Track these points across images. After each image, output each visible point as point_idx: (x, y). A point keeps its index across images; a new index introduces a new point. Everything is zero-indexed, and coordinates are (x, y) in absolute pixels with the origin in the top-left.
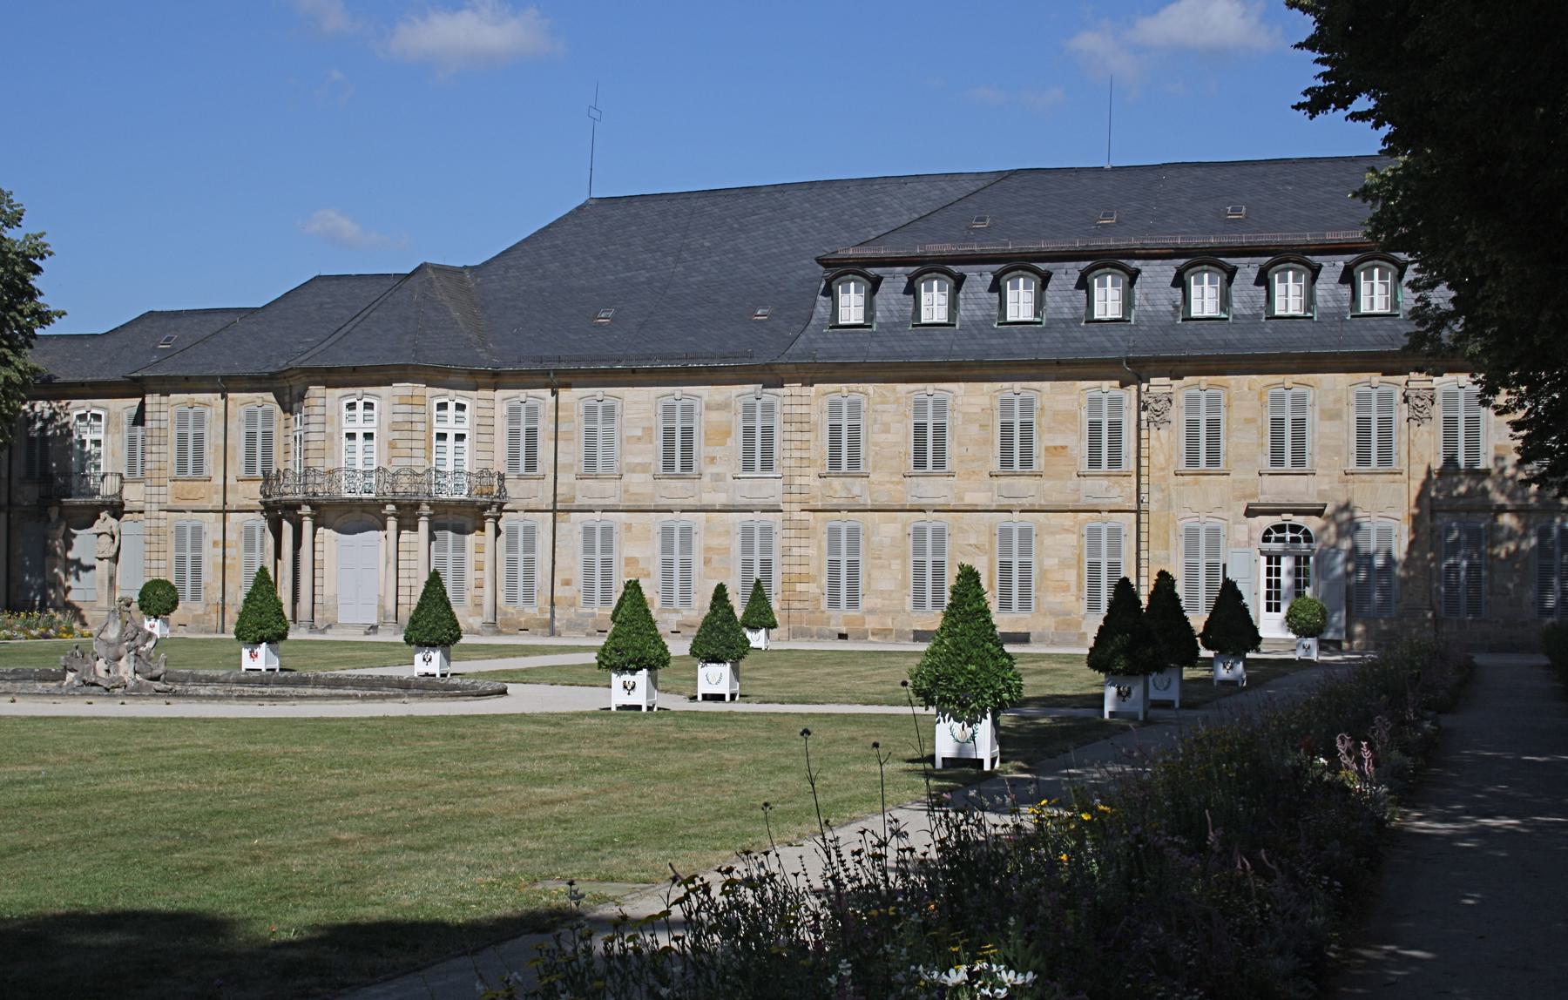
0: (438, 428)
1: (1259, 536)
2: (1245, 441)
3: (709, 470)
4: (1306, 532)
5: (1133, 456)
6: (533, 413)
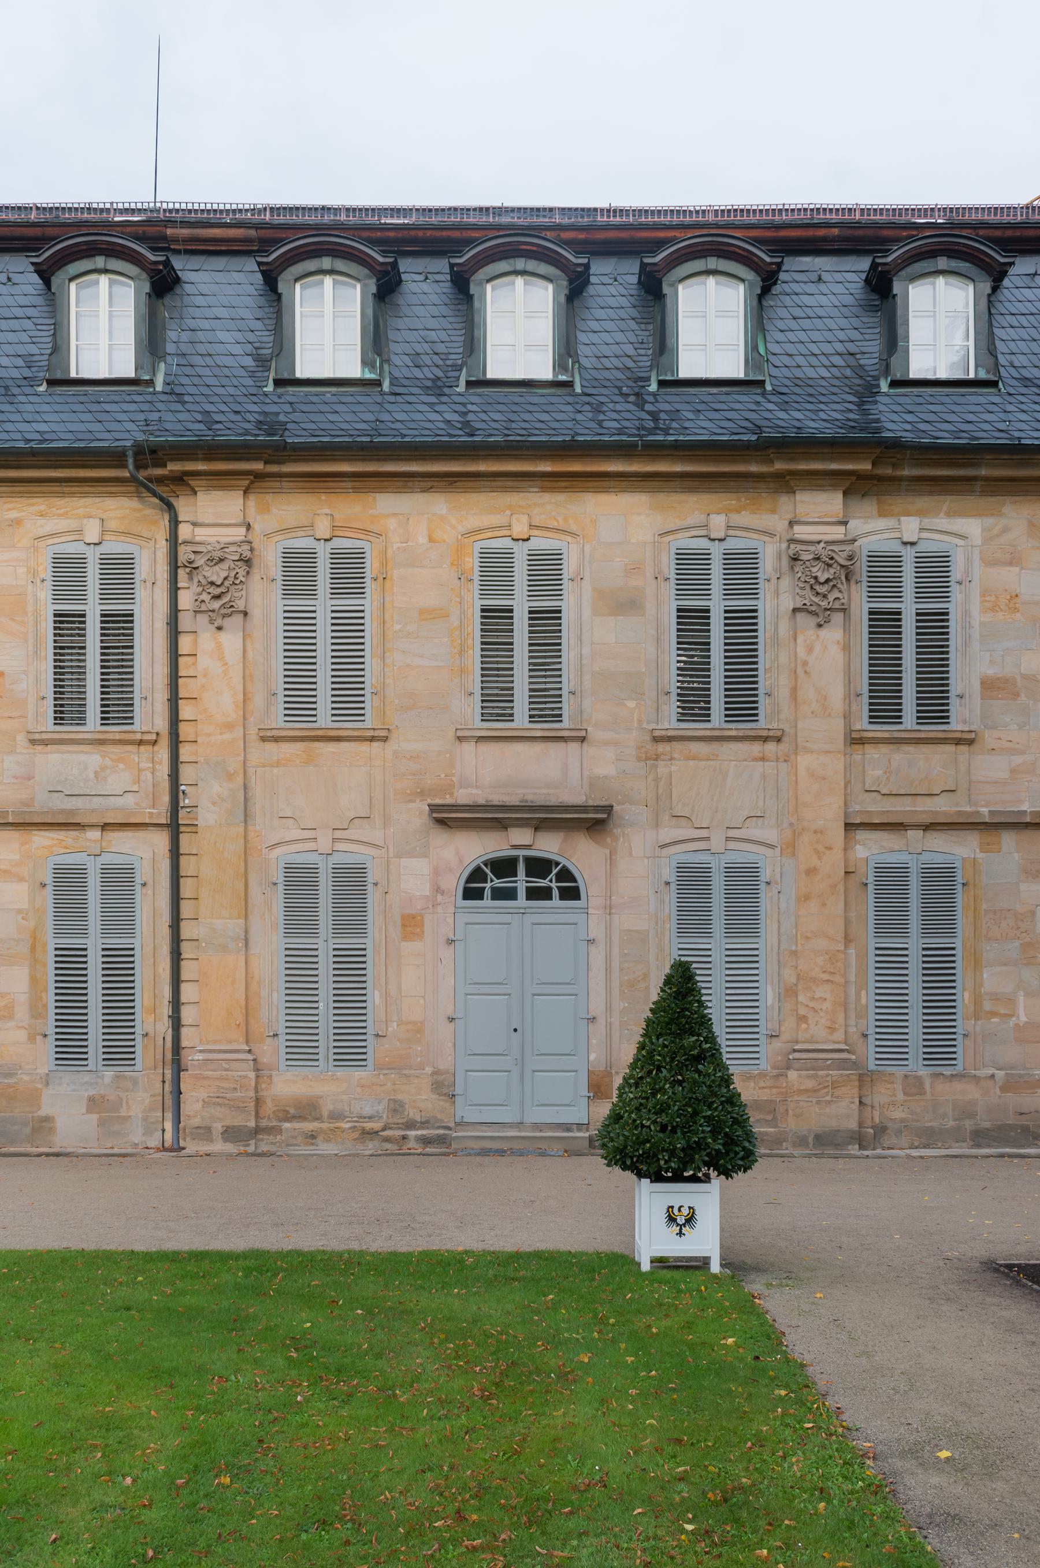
1: (455, 882)
4: (566, 875)
5: (161, 696)
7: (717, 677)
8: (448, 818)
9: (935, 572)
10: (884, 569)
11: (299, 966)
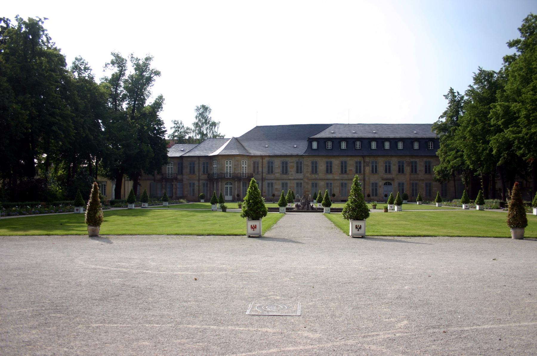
0: (242, 166)
2: (381, 169)
3: (290, 173)
6: (258, 163)
7: (401, 170)
8: (383, 179)
9: (416, 162)
10: (412, 162)
11: (373, 190)
